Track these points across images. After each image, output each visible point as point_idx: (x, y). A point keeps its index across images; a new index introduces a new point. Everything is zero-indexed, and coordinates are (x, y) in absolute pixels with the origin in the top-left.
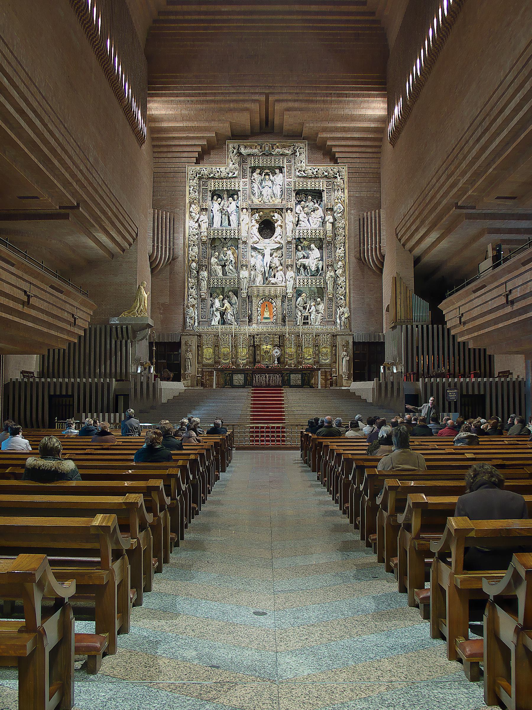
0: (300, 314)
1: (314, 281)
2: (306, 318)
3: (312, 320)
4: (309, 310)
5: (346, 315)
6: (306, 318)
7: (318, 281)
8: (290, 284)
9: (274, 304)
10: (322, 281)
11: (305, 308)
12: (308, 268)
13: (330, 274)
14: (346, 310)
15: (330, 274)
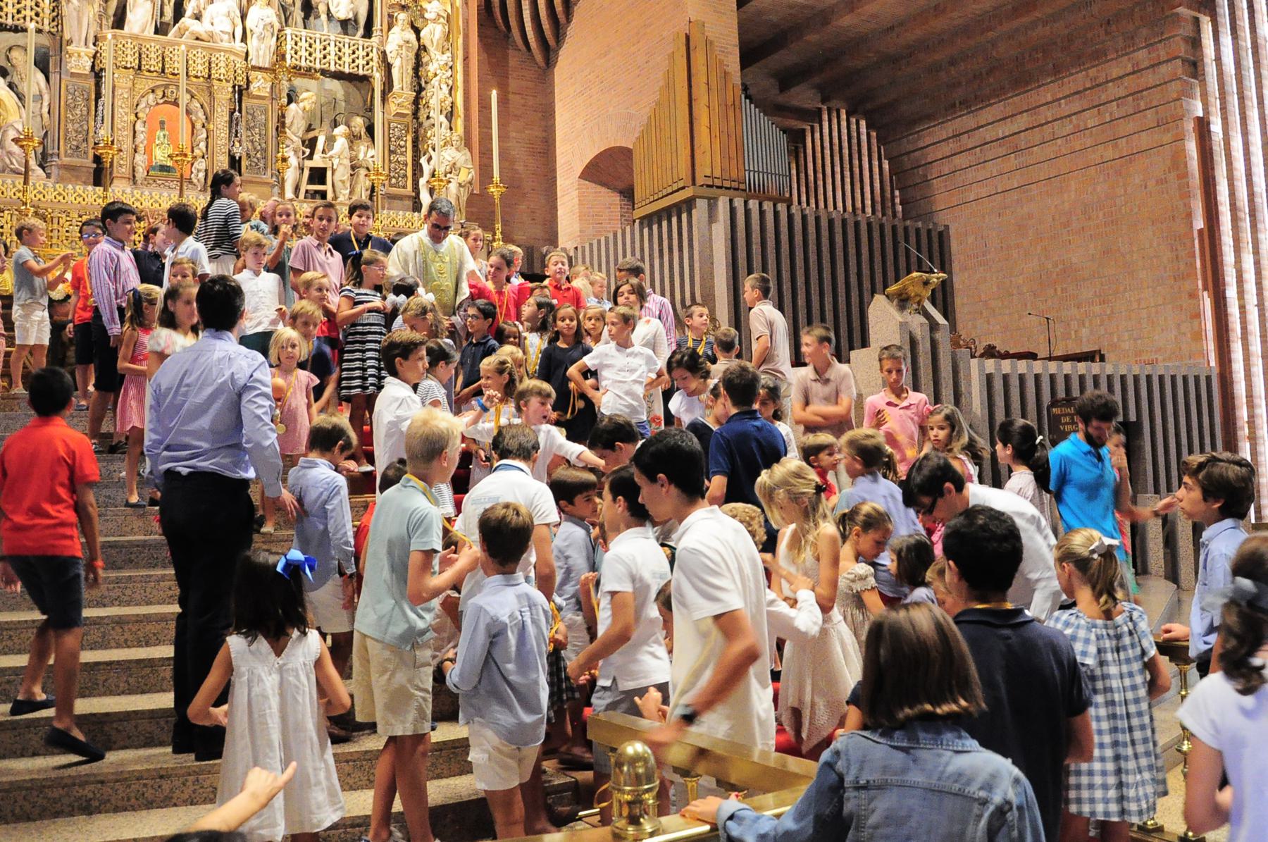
0: (293, 161)
1: (346, 50)
2: (318, 175)
3: (338, 185)
4: (324, 152)
5: (464, 176)
6: (318, 175)
7: (361, 53)
8: (261, 52)
9: (201, 114)
10: (374, 55)
11: (312, 144)
12: (322, 8)
13: (397, 40)
14: (461, 156)
15: (397, 40)
